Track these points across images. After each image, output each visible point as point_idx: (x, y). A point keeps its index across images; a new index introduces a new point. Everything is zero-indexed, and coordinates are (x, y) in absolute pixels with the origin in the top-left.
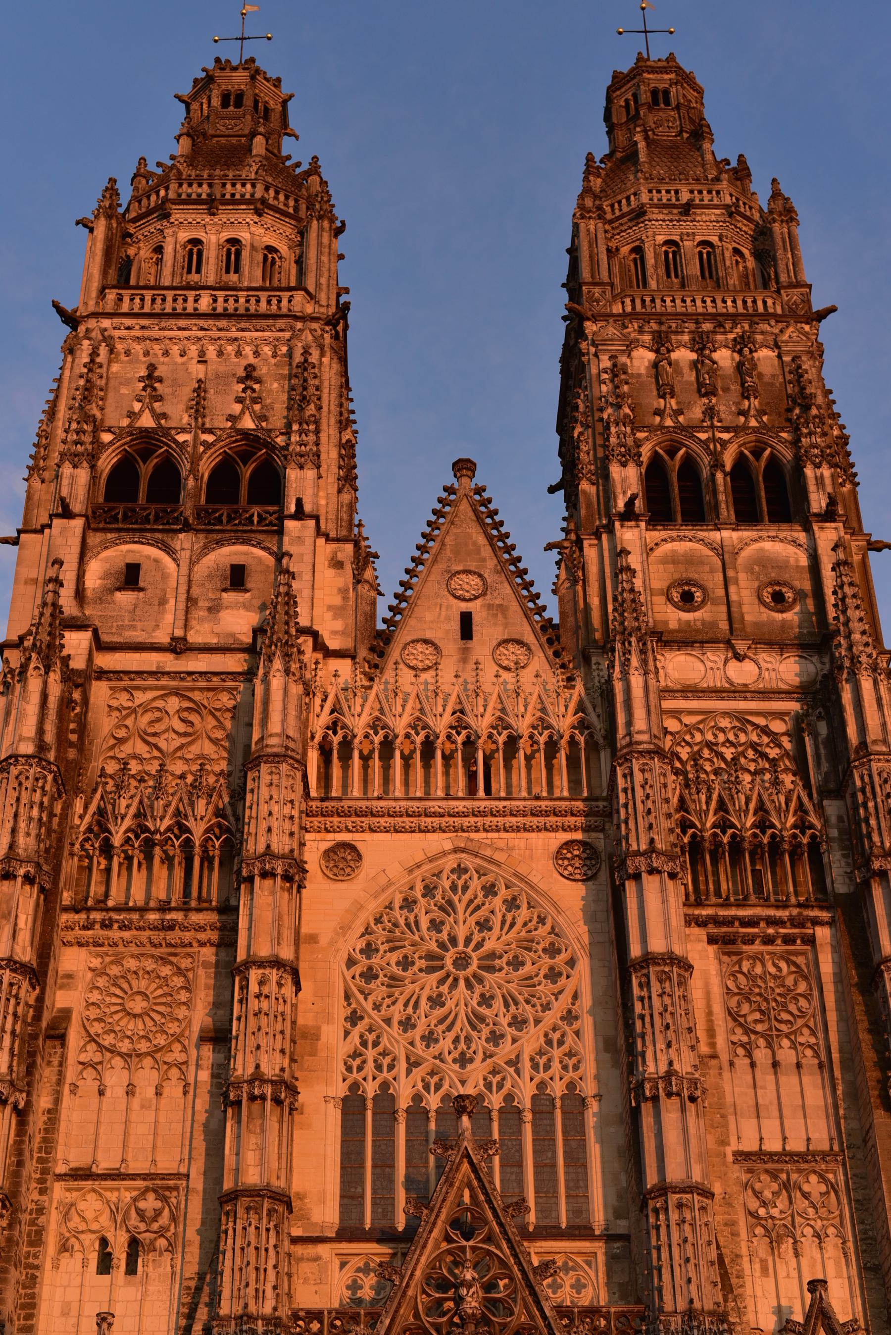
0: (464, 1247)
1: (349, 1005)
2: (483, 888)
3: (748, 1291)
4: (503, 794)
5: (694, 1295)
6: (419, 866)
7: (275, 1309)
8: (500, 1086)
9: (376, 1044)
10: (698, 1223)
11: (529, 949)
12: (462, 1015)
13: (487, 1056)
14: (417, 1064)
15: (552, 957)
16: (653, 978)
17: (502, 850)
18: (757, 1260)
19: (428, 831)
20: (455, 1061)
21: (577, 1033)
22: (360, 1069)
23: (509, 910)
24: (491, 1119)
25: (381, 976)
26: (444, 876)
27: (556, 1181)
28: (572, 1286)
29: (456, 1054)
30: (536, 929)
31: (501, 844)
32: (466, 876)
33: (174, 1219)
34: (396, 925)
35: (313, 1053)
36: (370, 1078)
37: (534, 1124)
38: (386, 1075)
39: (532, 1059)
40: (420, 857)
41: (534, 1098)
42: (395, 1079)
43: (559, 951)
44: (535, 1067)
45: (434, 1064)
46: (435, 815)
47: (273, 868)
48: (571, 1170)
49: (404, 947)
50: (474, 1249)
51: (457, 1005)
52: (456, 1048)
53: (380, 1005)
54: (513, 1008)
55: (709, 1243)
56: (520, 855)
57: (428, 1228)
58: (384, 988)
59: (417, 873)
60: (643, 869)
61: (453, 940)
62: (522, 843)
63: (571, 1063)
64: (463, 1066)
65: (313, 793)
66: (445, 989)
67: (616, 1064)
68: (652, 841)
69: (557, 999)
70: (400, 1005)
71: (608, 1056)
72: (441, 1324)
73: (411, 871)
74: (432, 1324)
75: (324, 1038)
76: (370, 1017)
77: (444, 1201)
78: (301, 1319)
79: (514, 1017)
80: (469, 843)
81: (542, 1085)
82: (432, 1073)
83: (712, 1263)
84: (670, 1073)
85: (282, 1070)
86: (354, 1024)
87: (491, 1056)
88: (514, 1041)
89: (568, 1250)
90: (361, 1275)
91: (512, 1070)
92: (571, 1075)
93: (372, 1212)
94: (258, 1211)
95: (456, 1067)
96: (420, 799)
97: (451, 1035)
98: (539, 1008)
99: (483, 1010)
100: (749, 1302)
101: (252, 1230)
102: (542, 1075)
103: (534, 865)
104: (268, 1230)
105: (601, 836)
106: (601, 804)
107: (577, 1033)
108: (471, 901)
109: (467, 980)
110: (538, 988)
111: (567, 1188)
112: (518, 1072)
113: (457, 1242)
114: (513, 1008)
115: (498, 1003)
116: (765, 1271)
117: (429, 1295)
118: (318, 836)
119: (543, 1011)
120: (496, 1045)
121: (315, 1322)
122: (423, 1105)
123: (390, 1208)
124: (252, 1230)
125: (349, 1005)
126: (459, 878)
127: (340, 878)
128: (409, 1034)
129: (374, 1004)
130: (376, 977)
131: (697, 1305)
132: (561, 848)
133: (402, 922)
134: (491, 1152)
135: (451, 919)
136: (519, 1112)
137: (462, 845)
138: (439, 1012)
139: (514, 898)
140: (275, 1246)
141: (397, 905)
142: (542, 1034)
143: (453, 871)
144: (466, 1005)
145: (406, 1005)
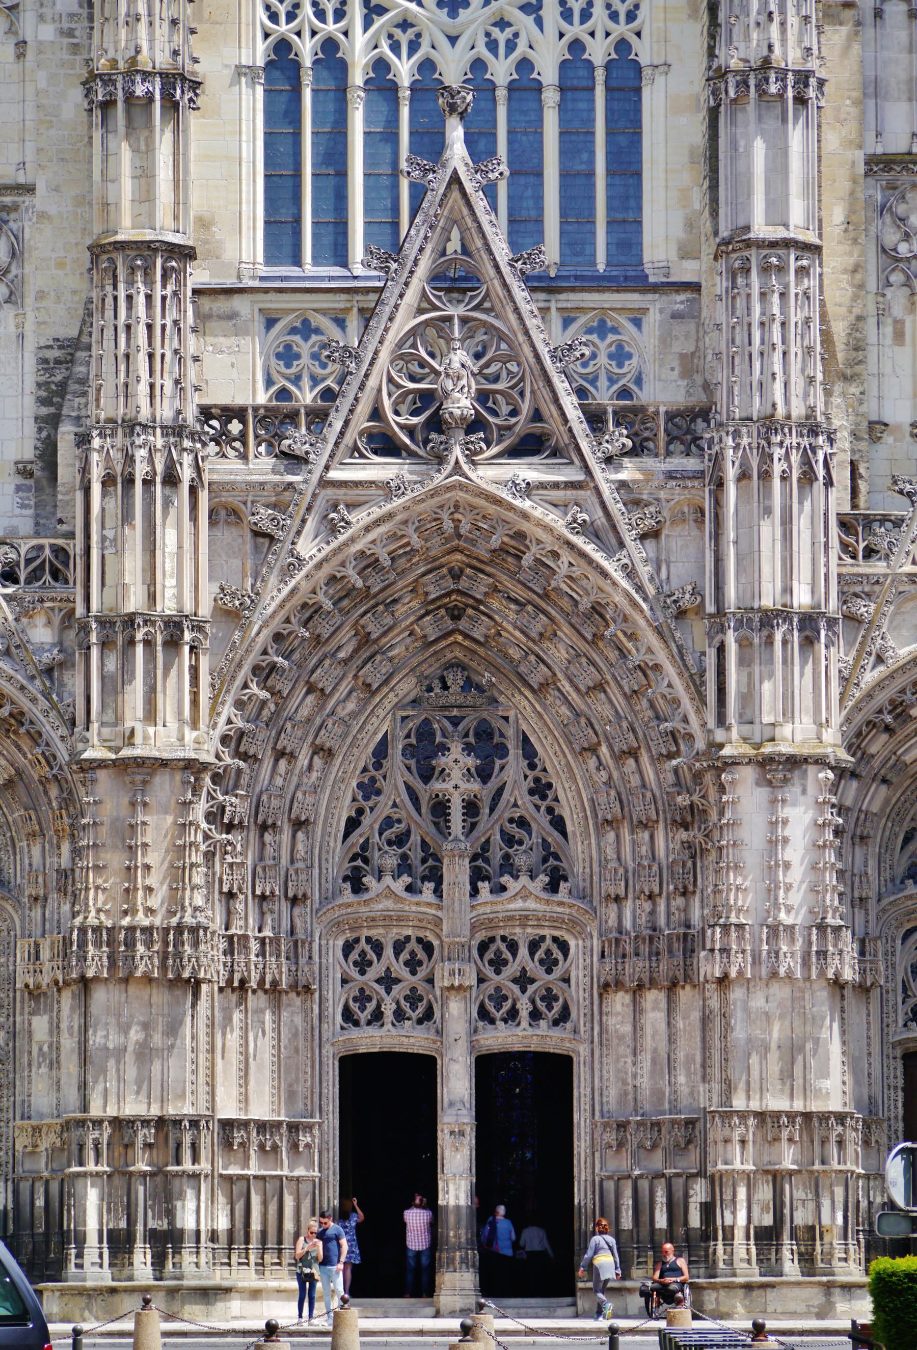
0: (449, 319)
3: (872, 367)
5: (779, 398)
7: (179, 412)
8: (511, 46)
10: (793, 291)
14: (381, 10)
18: (889, 321)
22: (291, 17)
24: (494, 100)
27: (592, 198)
28: (611, 356)
33: (13, 255)
36: (307, 34)
37: (562, 107)
38: (331, 27)
41: (564, 65)
42: (346, 34)
48: (617, 181)
50: (464, 321)
55: (807, 321)
57: (397, 292)
67: (694, 14)
72: (415, 425)
74: (402, 427)
77: (421, 250)
78: (213, 417)
81: (576, 46)
82: (405, 25)
83: (809, 351)
84: (766, 64)
85: (176, 53)
89: (606, 306)
90: (297, 338)
91: (528, 21)
92: (621, 29)
93: (314, 246)
94: (148, 272)
100: (872, 386)
101: (141, 300)
102: (576, 30)
104: (164, 298)
111: (610, 208)
112: (539, 22)
113: (438, 309)
116: (899, 336)
117: (399, 386)
121: (235, 421)
122: (390, 76)
123: (340, 239)
124: (141, 300)
131: (781, 411)
134: (490, 175)
136: (538, 88)
140: (176, 323)
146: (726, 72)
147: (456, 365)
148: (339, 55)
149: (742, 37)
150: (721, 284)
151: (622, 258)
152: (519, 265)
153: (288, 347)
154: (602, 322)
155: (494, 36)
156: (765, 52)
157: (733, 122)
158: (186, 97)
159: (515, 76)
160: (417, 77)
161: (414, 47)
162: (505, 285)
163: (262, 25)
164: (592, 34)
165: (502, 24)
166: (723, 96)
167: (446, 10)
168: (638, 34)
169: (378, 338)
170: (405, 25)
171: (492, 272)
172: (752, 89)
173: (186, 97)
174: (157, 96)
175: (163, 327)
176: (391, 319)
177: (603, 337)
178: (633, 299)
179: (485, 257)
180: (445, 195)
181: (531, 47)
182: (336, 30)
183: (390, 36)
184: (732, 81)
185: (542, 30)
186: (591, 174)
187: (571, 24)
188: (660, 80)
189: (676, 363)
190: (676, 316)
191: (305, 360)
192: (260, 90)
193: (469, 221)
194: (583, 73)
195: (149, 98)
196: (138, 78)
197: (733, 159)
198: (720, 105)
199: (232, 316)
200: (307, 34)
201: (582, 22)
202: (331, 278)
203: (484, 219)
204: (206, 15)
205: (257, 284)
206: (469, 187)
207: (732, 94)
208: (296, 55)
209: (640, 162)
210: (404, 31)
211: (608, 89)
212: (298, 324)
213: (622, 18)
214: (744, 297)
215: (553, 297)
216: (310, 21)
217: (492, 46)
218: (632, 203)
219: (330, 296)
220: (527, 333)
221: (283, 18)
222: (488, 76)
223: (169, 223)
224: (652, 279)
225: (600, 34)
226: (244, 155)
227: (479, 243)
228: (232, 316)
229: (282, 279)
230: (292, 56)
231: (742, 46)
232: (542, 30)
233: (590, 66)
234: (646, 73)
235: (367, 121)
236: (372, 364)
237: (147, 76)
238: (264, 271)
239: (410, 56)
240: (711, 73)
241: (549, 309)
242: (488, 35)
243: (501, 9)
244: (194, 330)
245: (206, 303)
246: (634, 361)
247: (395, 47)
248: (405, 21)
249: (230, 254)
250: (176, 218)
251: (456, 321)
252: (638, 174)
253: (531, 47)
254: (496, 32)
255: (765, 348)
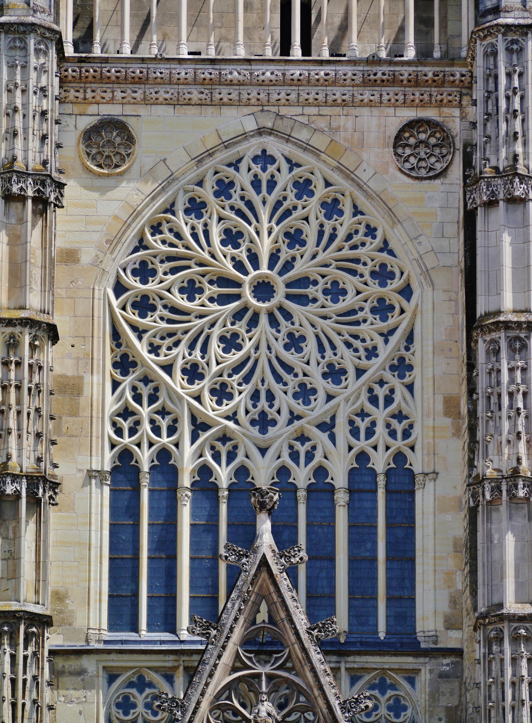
0: (258, 676)
1: (119, 345)
2: (296, 184)
4: (326, 55)
6: (210, 153)
8: (310, 456)
9: (153, 399)
11: (353, 272)
12: (263, 363)
13: (294, 417)
14: (205, 427)
15: (383, 284)
16: (503, 345)
17: (323, 131)
19: (223, 105)
20: (253, 423)
21: (410, 387)
22: (133, 431)
23: (328, 217)
25: (160, 307)
26: (243, 166)
27: (375, 579)
28: (389, 708)
29: (255, 413)
30: (363, 244)
31: (322, 123)
32: (271, 169)
34: (178, 236)
35: (74, 413)
36: (145, 445)
37: (350, 505)
38: (165, 440)
39: (351, 422)
40: (212, 142)
41: (352, 473)
42: (177, 445)
43: (392, 276)
44: (355, 432)
45: (226, 427)
46: (231, 83)
47: (21, 189)
49: (189, 267)
50: (270, 677)
51: (257, 348)
52: (255, 406)
53: (159, 347)
54: (329, 352)
56: (346, 140)
57: (216, 654)
58: (164, 325)
59: (209, 164)
60: (501, 196)
61: (254, 258)
62: (349, 123)
63: (399, 428)
64: (263, 431)
65: (69, 51)
66: (240, 327)
67: (457, 433)
68: (515, 158)
69: (386, 342)
70: (182, 348)
71: (448, 421)
73: (200, 161)
75: (87, 391)
76: (145, 364)
77: (236, 620)
79: (330, 365)
80: (279, 122)
82: (224, 438)
84: (515, 473)
85: (39, 460)
86: (125, 373)
87: (299, 418)
88: (330, 397)
89: (386, 666)
90: (134, 691)
91: (324, 437)
92: (398, 444)
93: (148, 616)
95: (255, 431)
96: (213, 61)
97: (248, 388)
98: (362, 353)
99: (290, 357)
102: (362, 444)
103: (365, 155)
104: (25, 658)
105: (456, 112)
106: (458, 70)
107: (410, 387)
108: (279, 204)
109: (271, 316)
110: (363, 326)
111: (388, 587)
112: (333, 438)
113: (250, 668)
114: (329, 352)
115: (310, 347)
118: (76, 109)
119: (368, 358)
120: (307, 402)
122: (212, 480)
125: (119, 345)
126: (264, 169)
127: (105, 171)
128: (195, 387)
129: (151, 345)
130: (154, 309)
132: (402, 130)
133: (187, 232)
135: (252, 230)
136: (331, 490)
137: (269, 125)
138: (235, 357)
139: (336, 201)
140: (35, 678)
141: (180, 208)
142: (364, 389)
143: (255, 159)
144: (269, 348)
145: (192, 347)
146: (483, 480)
147: (263, 714)
148: (172, 462)
149: (496, 452)
150: (479, 651)
151: (399, 628)
152: (315, 633)
153: (126, 698)
154: (383, 680)
155: (296, 448)
156: (515, 464)
157: (489, 519)
158: (47, 495)
159: (313, 481)
160: (234, 480)
161: (231, 456)
162: (304, 650)
163: (110, 438)
164: (375, 448)
165: (303, 438)
166: (481, 498)
167: (257, 427)
168: (412, 448)
169: (199, 691)
170: (224, 438)
171: (293, 638)
172: (504, 493)
173: (47, 495)
174: (24, 494)
175: (25, 681)
176: (211, 676)
177: (383, 693)
178: (408, 662)
179: (287, 626)
180: (255, 575)
181: (326, 457)
182: (169, 442)
183: (213, 448)
184: (488, 487)
185: (334, 444)
186: (374, 560)
187: (358, 439)
188: (430, 485)
189: (442, 715)
190: (443, 676)
191: (140, 709)
192: (107, 490)
193: (275, 597)
194: (367, 479)
195: (17, 496)
196: (9, 480)
197: (489, 550)
198: (478, 506)
199: (81, 672)
200: (145, 445)
201: (367, 438)
202: (162, 642)
203: (287, 595)
204: (64, 430)
205: (101, 646)
206: (275, 569)
207: (488, 497)
208: (136, 462)
209: (414, 550)
210: (224, 444)
211: (388, 491)
212: (135, 679)
213: (399, 435)
214: (498, 661)
215: (342, 659)
216: (148, 435)
217: (294, 456)
218: (407, 583)
219: (161, 657)
220: (321, 688)
221: (126, 433)
222: (291, 480)
223: (31, 596)
224: (423, 646)
225: (381, 448)
226: (93, 542)
227: (283, 615)
228: (81, 672)
229: (123, 642)
230: (133, 463)
231: (496, 459)
232: (334, 444)
233: (373, 473)
234: (419, 479)
235: (193, 515)
236: (194, 713)
237: (15, 478)
238: (107, 635)
239: (228, 464)
240: (471, 480)
241: (339, 669)
242: (291, 447)
243: (302, 427)
244: (50, 684)
245: (60, 662)
246: (409, 712)
247: (217, 457)
248: (224, 435)
249: (80, 622)
250: (37, 592)
251: (264, 678)
252: (412, 560)
253: (326, 457)
254: (298, 445)
255: (516, 703)
